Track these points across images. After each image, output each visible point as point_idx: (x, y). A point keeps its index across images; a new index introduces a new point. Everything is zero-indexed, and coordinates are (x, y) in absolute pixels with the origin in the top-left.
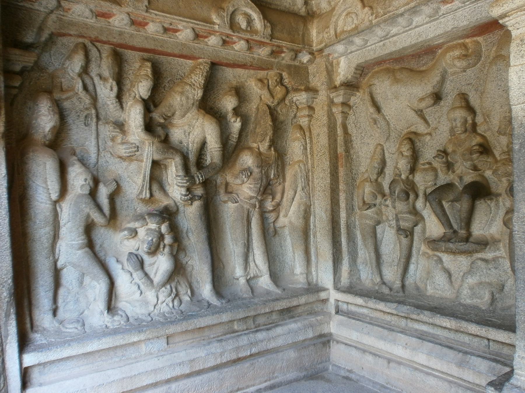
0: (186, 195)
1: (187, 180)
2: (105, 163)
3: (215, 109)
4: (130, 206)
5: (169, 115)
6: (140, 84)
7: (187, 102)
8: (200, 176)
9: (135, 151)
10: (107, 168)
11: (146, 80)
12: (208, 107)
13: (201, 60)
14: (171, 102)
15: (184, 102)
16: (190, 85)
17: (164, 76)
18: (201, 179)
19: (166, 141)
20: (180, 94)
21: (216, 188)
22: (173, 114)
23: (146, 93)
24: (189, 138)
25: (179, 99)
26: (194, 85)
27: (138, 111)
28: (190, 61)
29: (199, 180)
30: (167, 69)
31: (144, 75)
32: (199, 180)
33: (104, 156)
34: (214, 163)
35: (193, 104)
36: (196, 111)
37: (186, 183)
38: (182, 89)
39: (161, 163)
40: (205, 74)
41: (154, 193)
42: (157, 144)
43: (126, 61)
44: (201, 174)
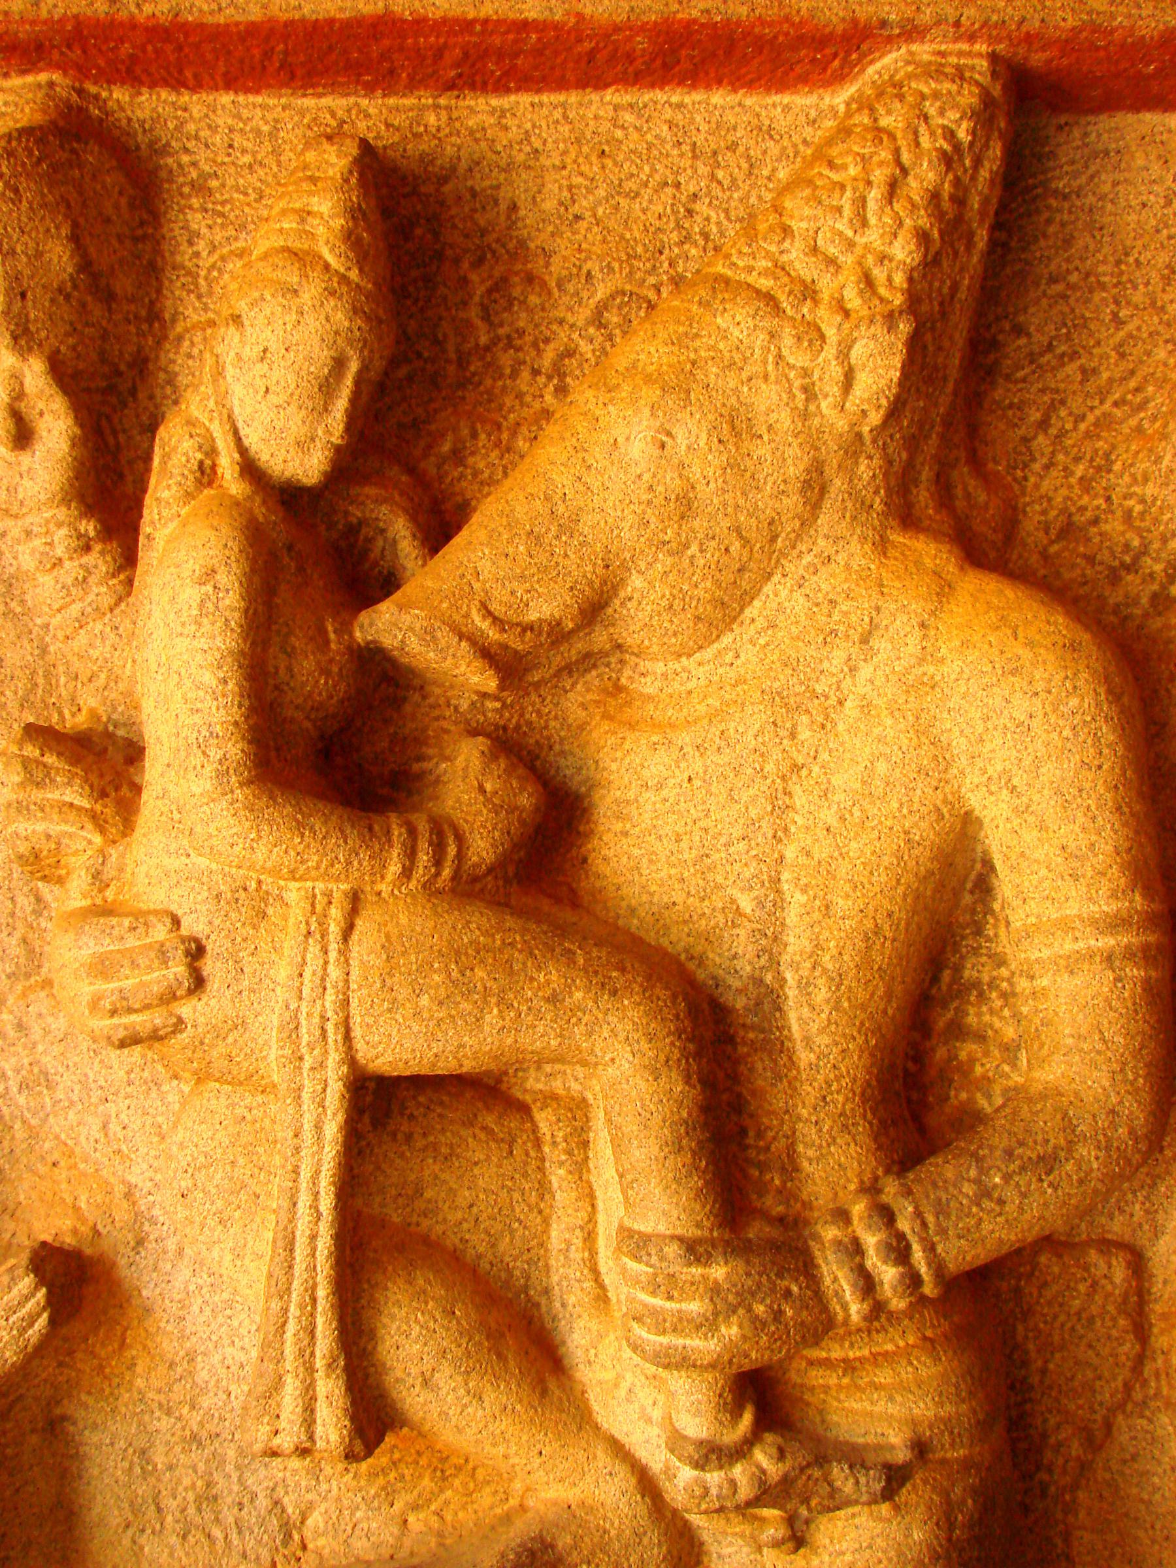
0: (711, 1454)
1: (715, 1290)
2: (23, 1086)
3: (1113, 526)
4: (227, 1487)
5: (540, 610)
6: (231, 345)
7: (737, 468)
8: (871, 1240)
9: (169, 997)
10: (33, 1134)
11: (273, 305)
12: (1030, 525)
13: (888, 62)
14: (563, 480)
15: (707, 470)
16: (769, 298)
17: (557, 267)
18: (888, 1274)
19: (542, 866)
20: (651, 394)
21: (1141, 1331)
22: (595, 608)
23: (295, 423)
24: (780, 835)
25: (638, 449)
26: (808, 292)
27: (191, 594)
28: (803, 101)
29: (867, 1284)
30: (584, 204)
31: (265, 257)
32: (867, 1284)
33: (20, 1026)
34: (1052, 1092)
35: (814, 487)
36: (857, 553)
37: (707, 1325)
38: (678, 342)
39: (535, 1082)
40: (925, 175)
41: (413, 1399)
42: (401, 909)
43: (200, 188)
44: (888, 1216)
